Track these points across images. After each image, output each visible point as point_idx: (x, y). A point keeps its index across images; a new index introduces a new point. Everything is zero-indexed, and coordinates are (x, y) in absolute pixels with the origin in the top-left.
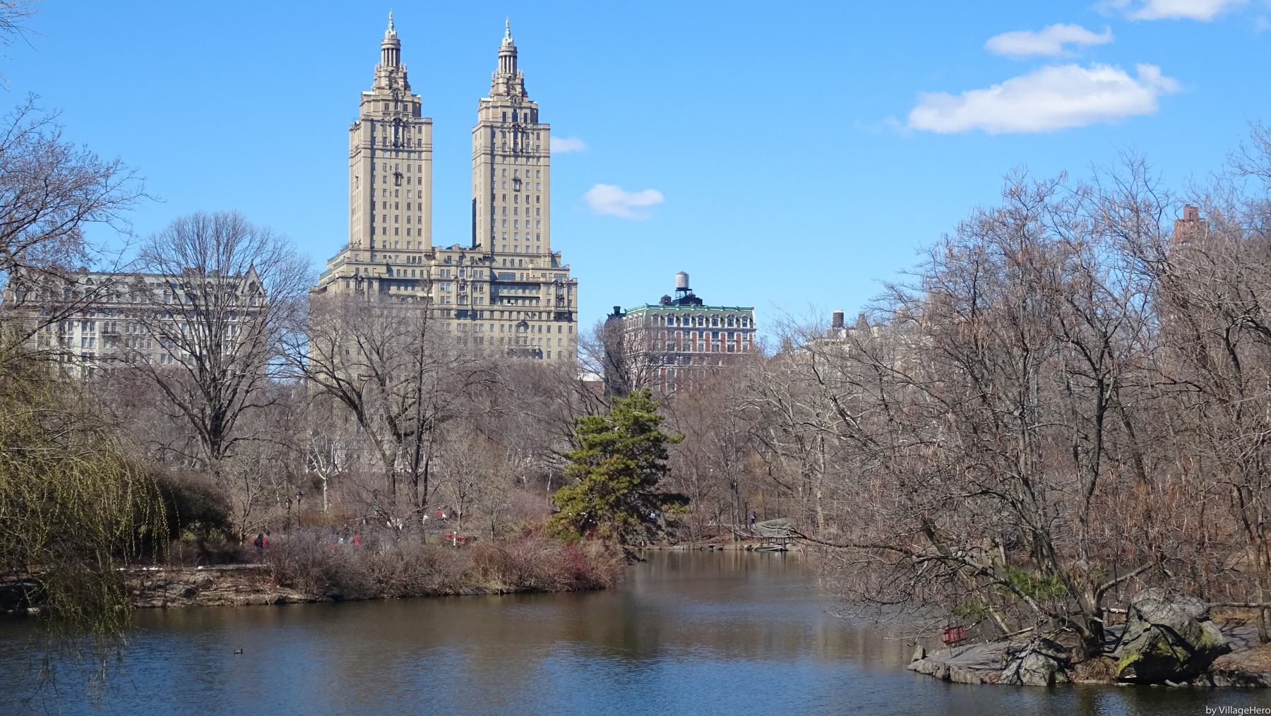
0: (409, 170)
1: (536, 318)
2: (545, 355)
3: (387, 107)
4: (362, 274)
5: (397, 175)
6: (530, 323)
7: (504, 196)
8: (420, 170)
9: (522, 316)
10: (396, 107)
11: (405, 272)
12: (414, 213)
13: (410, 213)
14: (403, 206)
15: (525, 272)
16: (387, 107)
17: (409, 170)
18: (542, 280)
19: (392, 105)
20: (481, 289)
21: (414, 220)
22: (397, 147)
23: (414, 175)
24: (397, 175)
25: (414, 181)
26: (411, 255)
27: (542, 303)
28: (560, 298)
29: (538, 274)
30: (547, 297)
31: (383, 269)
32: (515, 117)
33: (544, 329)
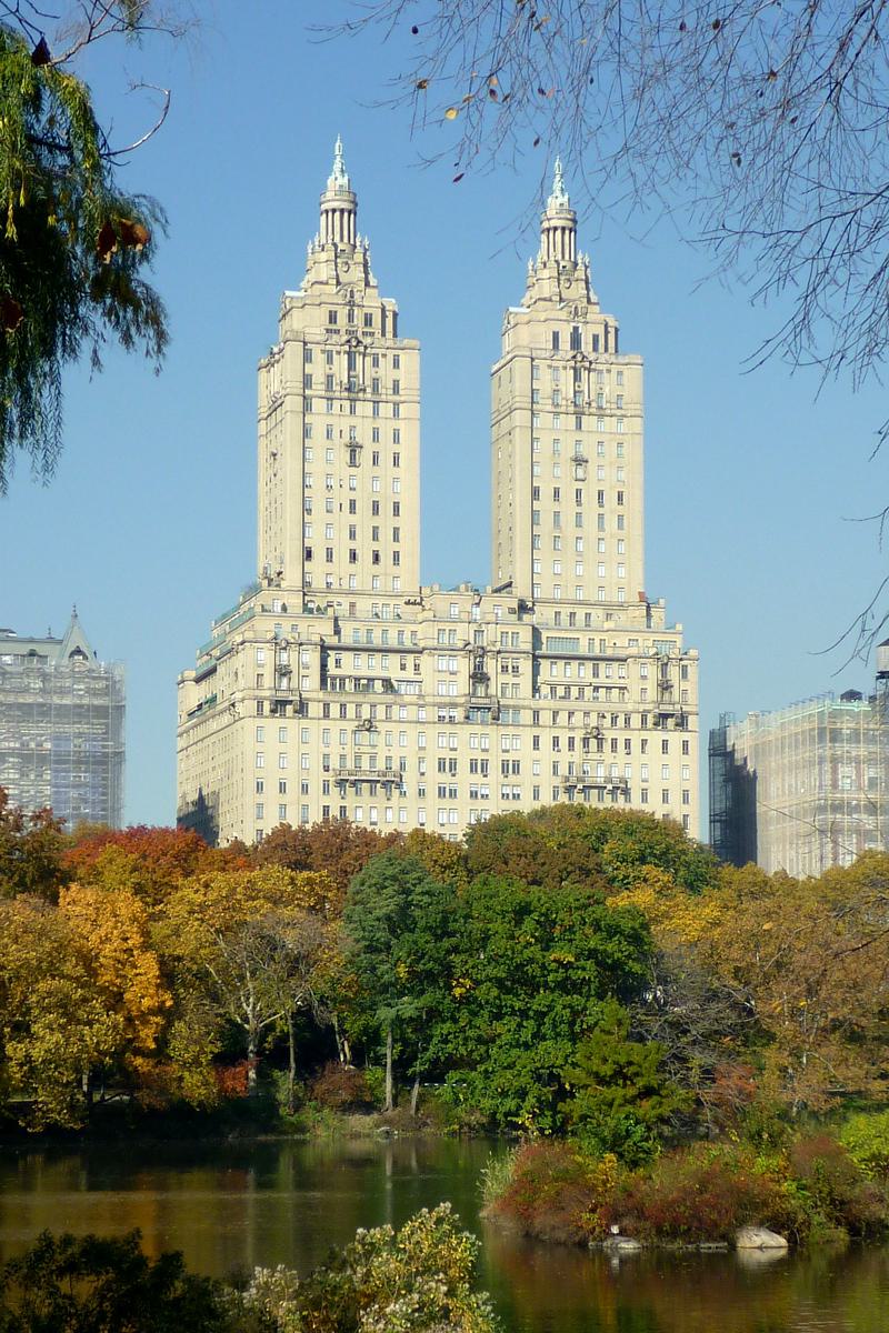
0: (376, 438)
1: (621, 721)
2: (636, 795)
3: (333, 318)
4: (286, 633)
6: (609, 735)
7: (557, 492)
8: (396, 439)
9: (593, 720)
10: (351, 317)
11: (369, 631)
12: (386, 521)
13: (376, 521)
14: (364, 507)
15: (597, 637)
16: (333, 318)
17: (376, 438)
18: (633, 651)
19: (342, 313)
20: (516, 669)
21: (386, 534)
23: (386, 448)
24: (354, 448)
25: (386, 459)
27: (633, 695)
29: (622, 640)
31: (328, 628)
32: (576, 341)
33: (636, 746)
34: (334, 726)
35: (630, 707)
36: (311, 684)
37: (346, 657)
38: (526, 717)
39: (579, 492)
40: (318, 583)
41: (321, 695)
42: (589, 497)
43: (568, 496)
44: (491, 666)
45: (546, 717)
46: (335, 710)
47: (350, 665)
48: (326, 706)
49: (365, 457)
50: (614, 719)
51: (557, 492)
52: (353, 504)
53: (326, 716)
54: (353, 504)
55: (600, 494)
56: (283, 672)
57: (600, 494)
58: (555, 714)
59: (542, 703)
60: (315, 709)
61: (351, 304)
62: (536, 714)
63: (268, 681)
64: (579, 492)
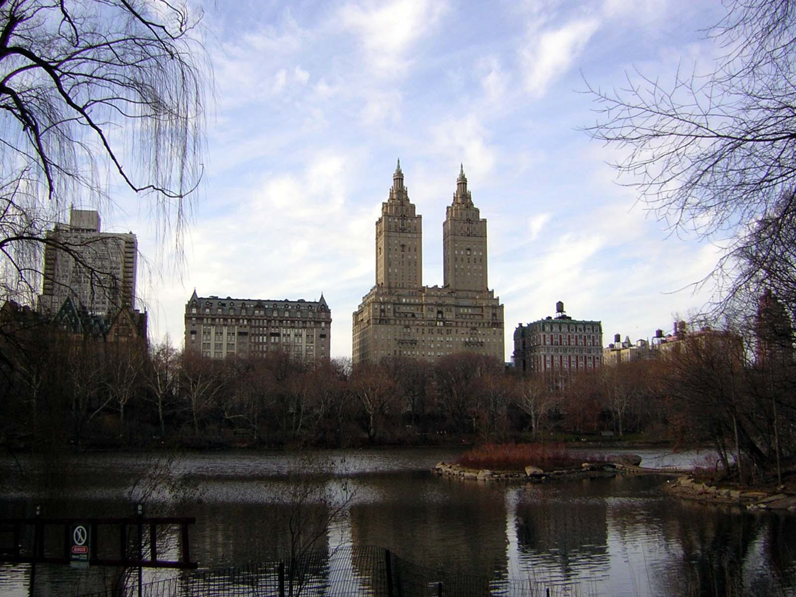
9: (474, 325)
10: (402, 209)
22: (403, 230)
26: (411, 291)
28: (494, 315)
30: (488, 315)
34: (398, 328)
35: (484, 321)
36: (390, 315)
37: (401, 307)
38: (454, 324)
40: (393, 285)
41: (394, 318)
44: (444, 310)
45: (460, 324)
46: (398, 322)
47: (404, 309)
49: (407, 249)
50: (480, 324)
51: (462, 260)
52: (403, 262)
53: (395, 324)
54: (403, 262)
56: (382, 311)
57: (475, 259)
58: (462, 322)
59: (459, 320)
60: (392, 322)
61: (402, 205)
62: (457, 323)
63: (378, 314)
64: (469, 258)
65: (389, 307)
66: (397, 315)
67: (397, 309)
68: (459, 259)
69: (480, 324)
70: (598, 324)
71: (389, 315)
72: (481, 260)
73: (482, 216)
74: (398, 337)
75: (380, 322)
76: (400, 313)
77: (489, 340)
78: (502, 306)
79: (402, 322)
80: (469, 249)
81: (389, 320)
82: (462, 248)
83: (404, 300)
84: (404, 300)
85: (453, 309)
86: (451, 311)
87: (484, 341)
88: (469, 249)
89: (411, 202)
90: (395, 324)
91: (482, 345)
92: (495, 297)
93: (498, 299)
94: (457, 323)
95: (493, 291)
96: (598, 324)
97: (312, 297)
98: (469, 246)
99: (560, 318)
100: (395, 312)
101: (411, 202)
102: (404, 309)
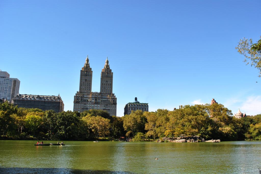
5: (86, 80)
24: (86, 80)
39: (107, 84)
42: (108, 84)
43: (106, 84)
45: (102, 103)
46: (82, 103)
48: (81, 102)
49: (87, 81)
50: (109, 104)
51: (105, 84)
55: (109, 84)
57: (109, 84)
58: (103, 103)
60: (80, 103)
62: (101, 103)
64: (107, 84)
65: (80, 98)
66: (82, 100)
67: (82, 99)
68: (104, 84)
69: (109, 104)
70: (147, 104)
71: (80, 100)
72: (111, 85)
73: (112, 72)
74: (82, 107)
75: (76, 103)
76: (83, 100)
77: (111, 109)
78: (116, 99)
79: (84, 103)
80: (107, 81)
81: (79, 102)
82: (105, 81)
83: (85, 96)
84: (85, 96)
85: (100, 99)
86: (100, 99)
87: (110, 109)
88: (107, 81)
89: (90, 67)
90: (81, 103)
91: (109, 110)
92: (115, 96)
93: (115, 96)
94: (101, 103)
95: (114, 94)
96: (147, 104)
97: (56, 95)
98: (107, 80)
99: (136, 102)
100: (81, 100)
101: (90, 67)
102: (85, 99)
